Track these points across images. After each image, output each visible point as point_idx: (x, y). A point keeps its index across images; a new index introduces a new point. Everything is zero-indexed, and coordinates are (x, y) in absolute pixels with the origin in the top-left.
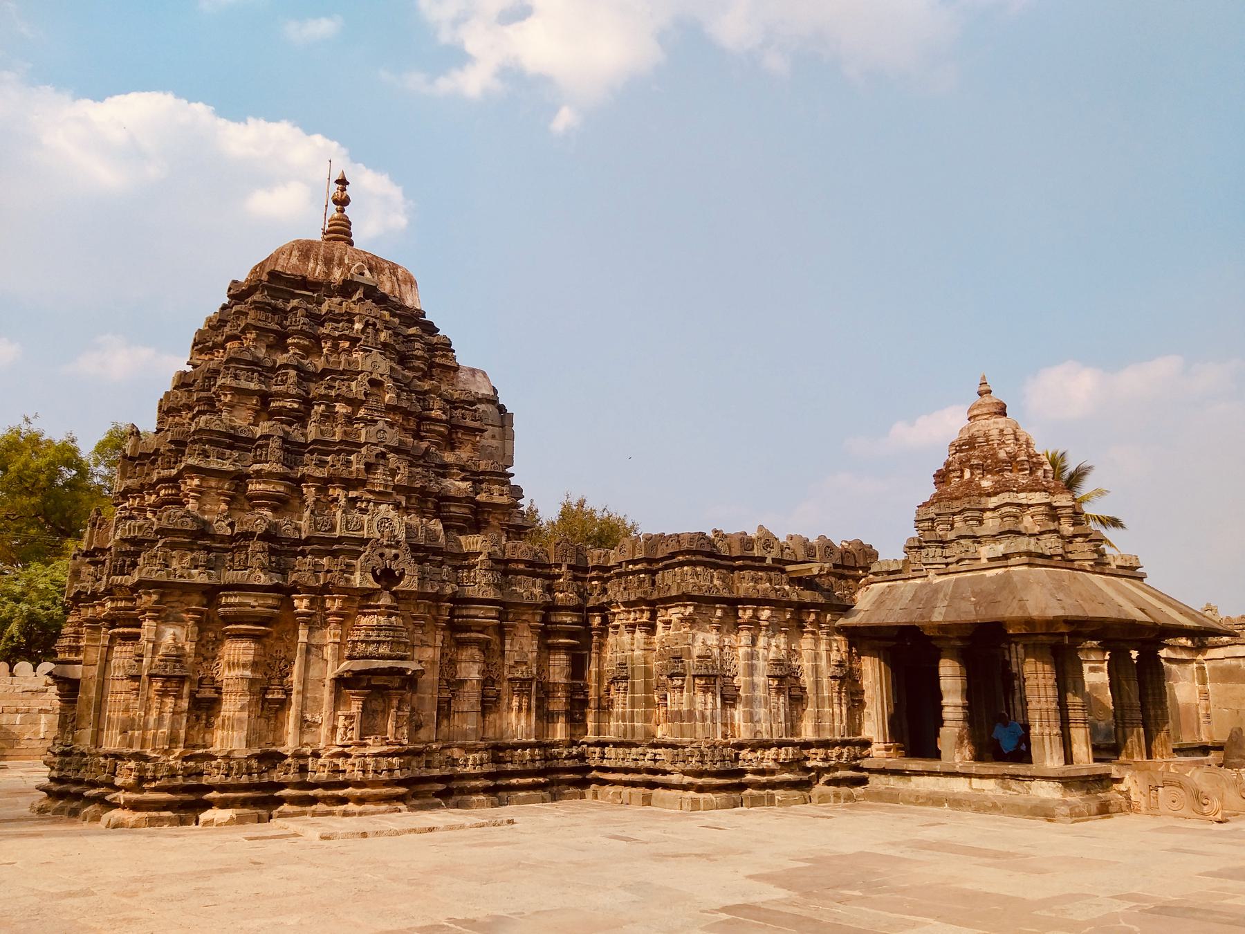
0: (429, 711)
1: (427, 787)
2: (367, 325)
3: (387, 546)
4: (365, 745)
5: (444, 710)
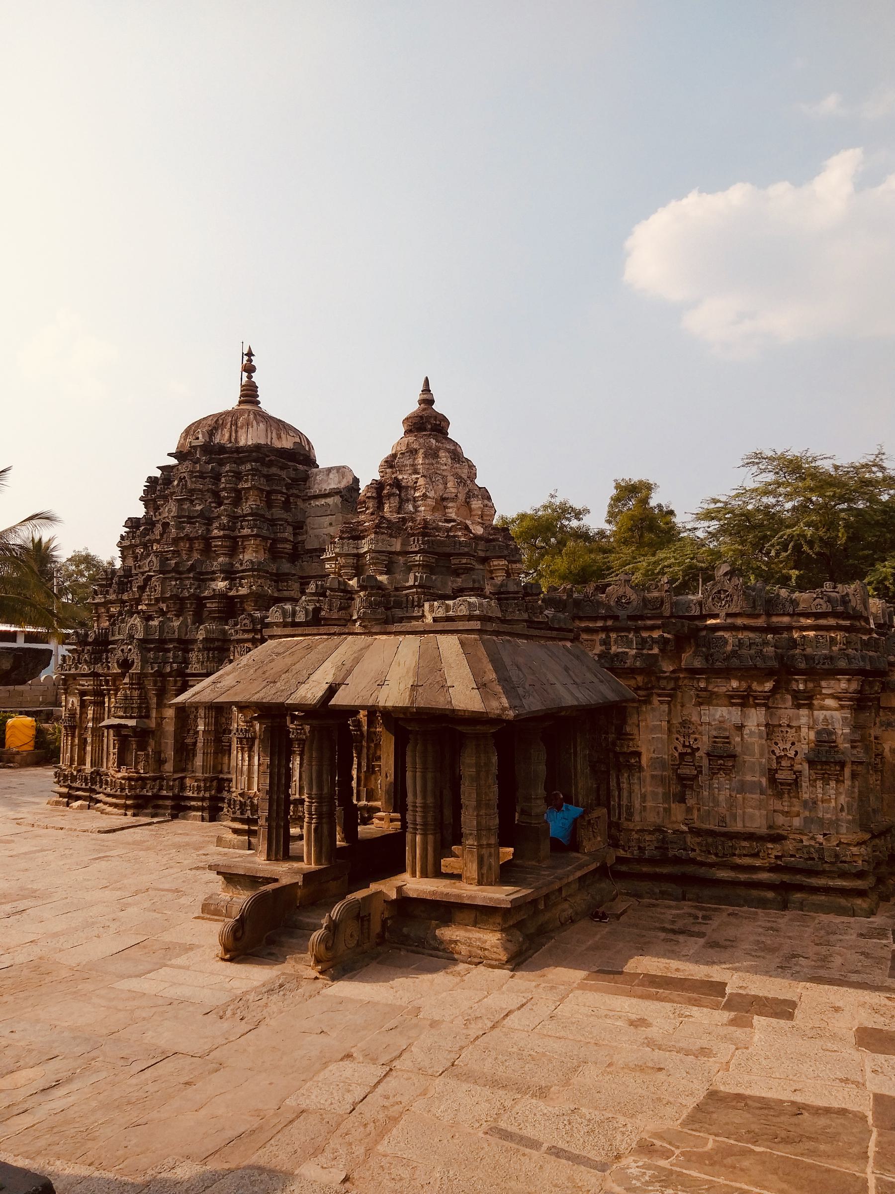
0: (169, 753)
1: (160, 802)
2: (181, 480)
3: (126, 644)
4: (119, 771)
5: (184, 752)
